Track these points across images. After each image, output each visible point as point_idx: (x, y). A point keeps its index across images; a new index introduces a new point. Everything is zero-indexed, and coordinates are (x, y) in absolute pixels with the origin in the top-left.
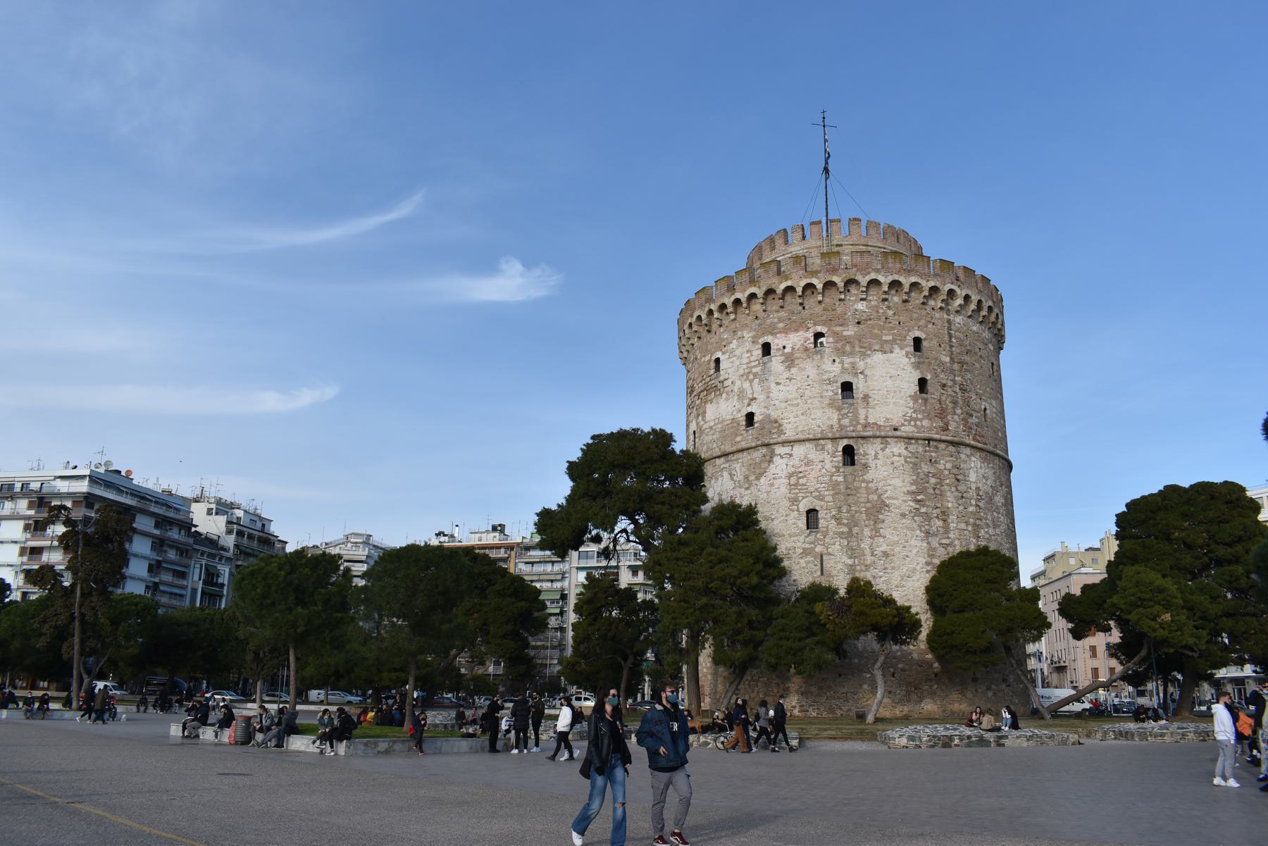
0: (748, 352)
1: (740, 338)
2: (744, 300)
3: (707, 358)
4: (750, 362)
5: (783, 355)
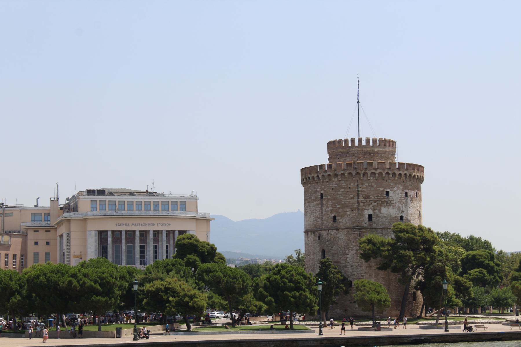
0: (401, 193)
1: (398, 187)
2: (403, 175)
3: (382, 189)
4: (402, 197)
5: (411, 198)
